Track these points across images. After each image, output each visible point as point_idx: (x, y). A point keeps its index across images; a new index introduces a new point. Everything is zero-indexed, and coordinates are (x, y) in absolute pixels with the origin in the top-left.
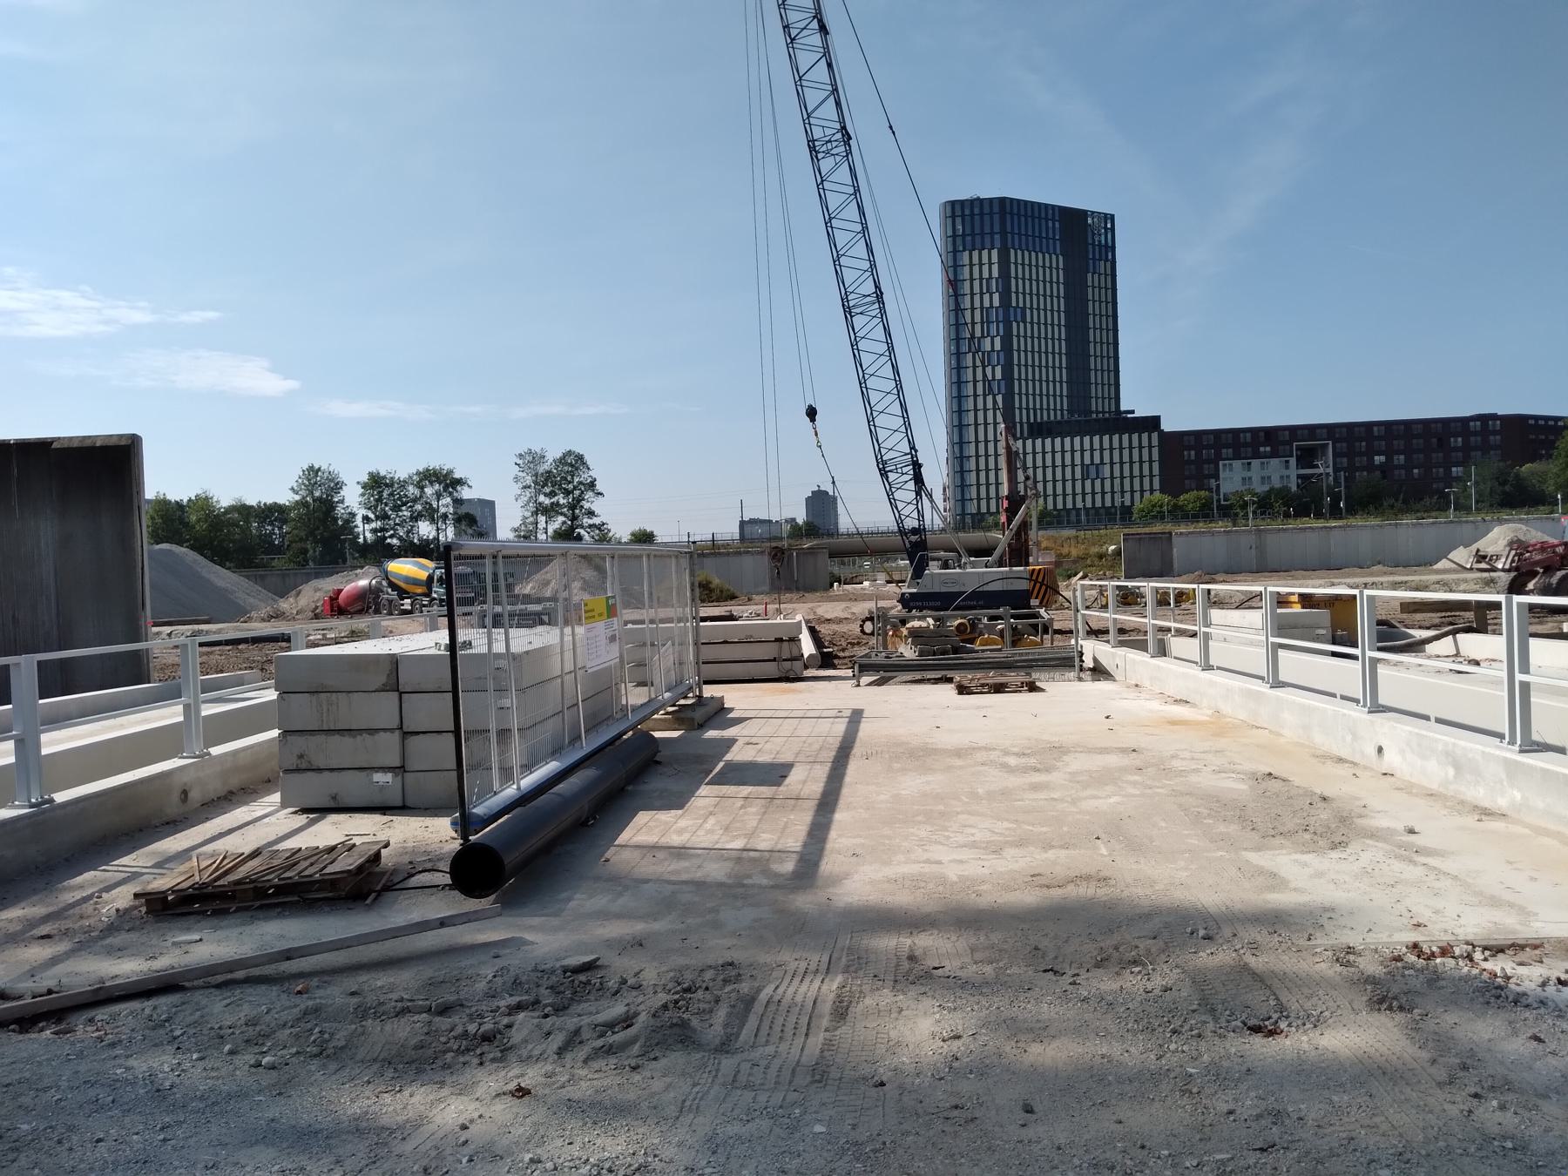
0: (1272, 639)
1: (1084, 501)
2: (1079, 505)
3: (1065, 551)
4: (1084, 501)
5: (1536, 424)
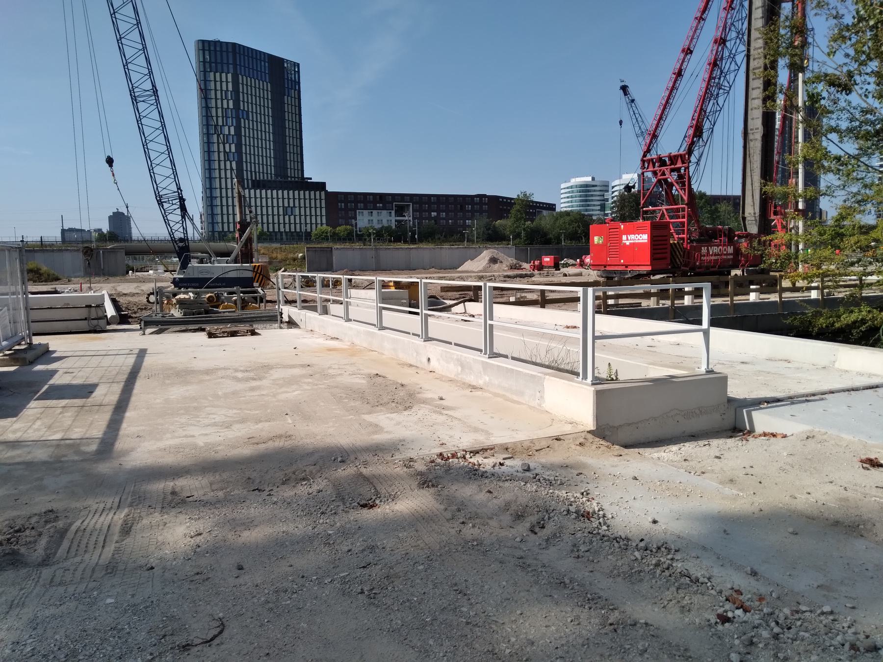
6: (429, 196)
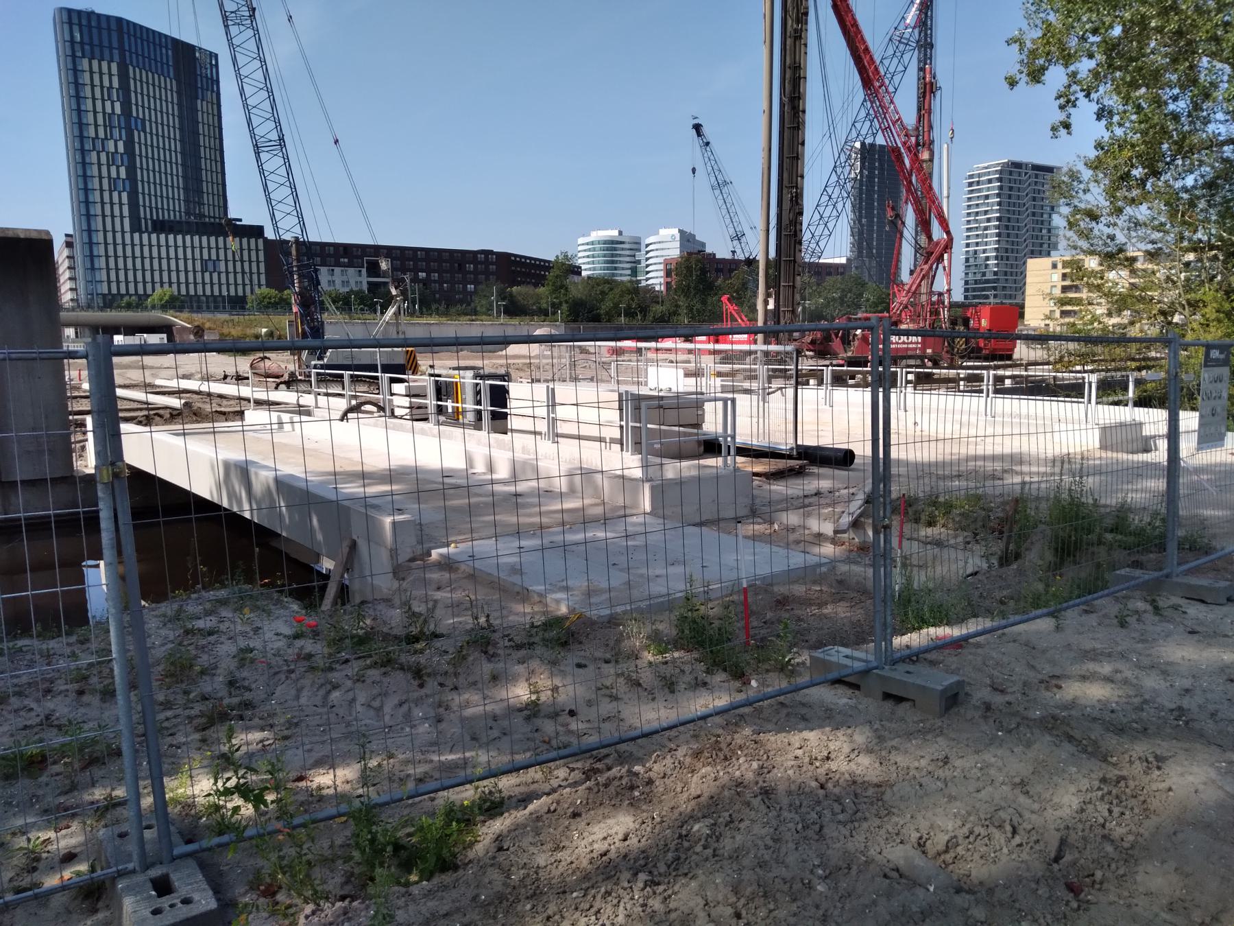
0: (381, 396)
1: (228, 291)
2: (225, 293)
3: (225, 331)
4: (228, 291)
5: (539, 265)
6: (451, 252)
